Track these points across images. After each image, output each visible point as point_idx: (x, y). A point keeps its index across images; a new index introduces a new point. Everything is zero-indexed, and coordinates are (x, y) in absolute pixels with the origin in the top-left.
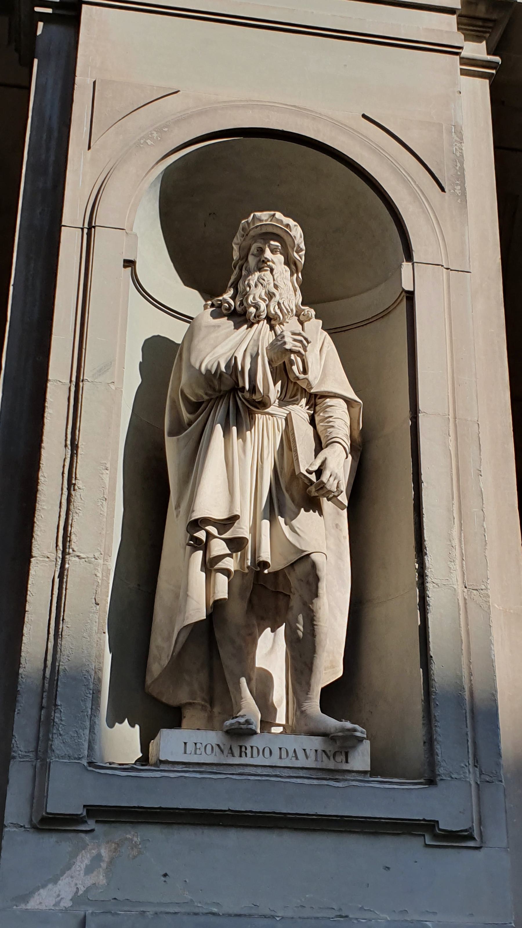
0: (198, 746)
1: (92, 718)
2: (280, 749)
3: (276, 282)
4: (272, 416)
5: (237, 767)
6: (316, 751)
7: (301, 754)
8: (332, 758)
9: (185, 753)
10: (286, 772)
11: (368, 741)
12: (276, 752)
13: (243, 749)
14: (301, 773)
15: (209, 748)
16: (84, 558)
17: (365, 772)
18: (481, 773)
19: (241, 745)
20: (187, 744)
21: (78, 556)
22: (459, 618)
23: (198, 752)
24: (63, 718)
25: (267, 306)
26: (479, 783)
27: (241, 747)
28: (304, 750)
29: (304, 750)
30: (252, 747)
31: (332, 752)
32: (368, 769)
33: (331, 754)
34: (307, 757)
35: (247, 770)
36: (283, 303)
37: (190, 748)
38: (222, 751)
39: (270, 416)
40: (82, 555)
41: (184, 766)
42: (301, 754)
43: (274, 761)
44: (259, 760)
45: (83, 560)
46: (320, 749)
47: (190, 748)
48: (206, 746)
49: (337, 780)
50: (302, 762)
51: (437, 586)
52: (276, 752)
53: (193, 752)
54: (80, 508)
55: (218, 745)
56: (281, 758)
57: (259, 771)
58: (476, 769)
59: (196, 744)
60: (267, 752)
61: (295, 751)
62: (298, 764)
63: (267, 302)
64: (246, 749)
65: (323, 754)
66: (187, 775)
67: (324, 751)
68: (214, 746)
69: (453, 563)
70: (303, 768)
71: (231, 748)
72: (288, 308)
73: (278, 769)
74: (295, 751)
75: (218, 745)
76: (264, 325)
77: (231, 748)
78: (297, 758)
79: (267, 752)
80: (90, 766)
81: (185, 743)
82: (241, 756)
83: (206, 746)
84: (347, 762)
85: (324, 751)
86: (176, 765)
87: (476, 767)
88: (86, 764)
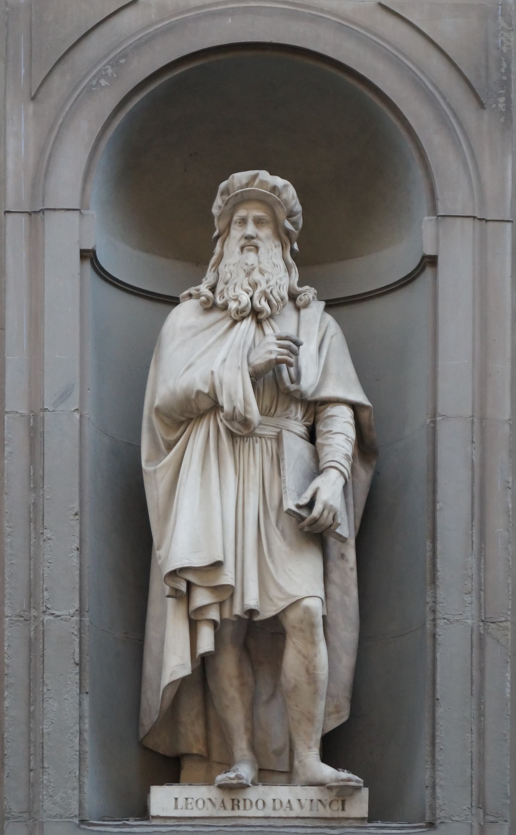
0: (190, 801)
1: (82, 778)
2: (274, 800)
3: (262, 266)
4: (260, 437)
5: (229, 819)
6: (312, 800)
7: (295, 805)
8: (328, 807)
9: (176, 807)
10: (280, 823)
11: (367, 789)
12: (269, 803)
13: (236, 802)
14: (297, 823)
15: (200, 803)
16: (59, 616)
17: (363, 819)
18: (485, 814)
19: (233, 798)
20: (179, 800)
21: (53, 614)
22: (472, 656)
23: (189, 806)
24: (52, 780)
25: (251, 298)
26: (482, 824)
27: (233, 800)
28: (299, 800)
29: (299, 800)
30: (245, 800)
31: (329, 801)
32: (366, 815)
33: (327, 804)
34: (302, 807)
35: (240, 822)
36: (271, 292)
37: (181, 803)
38: (214, 805)
39: (258, 439)
40: (57, 613)
41: (176, 820)
42: (295, 805)
43: (269, 812)
44: (253, 812)
45: (58, 618)
46: (315, 798)
47: (181, 803)
48: (197, 801)
49: (332, 828)
50: (297, 811)
51: (448, 623)
52: (269, 803)
53: (184, 807)
54: (50, 561)
55: (210, 799)
56: (274, 809)
57: (253, 822)
58: (481, 811)
59: (187, 799)
60: (260, 804)
61: (289, 801)
62: (293, 814)
63: (251, 294)
64: (239, 802)
65: (320, 804)
66: (179, 829)
67: (320, 801)
68: (206, 800)
69: (468, 596)
70: (297, 818)
71: (223, 802)
72: (278, 297)
73: (272, 820)
74: (289, 801)
75: (210, 799)
76: (247, 326)
77: (223, 802)
78: (291, 808)
79: (260, 804)
80: (83, 824)
81: (176, 799)
82: (233, 809)
83: (197, 801)
84: (343, 809)
85: (320, 801)
86: (168, 820)
87: (481, 808)
88: (77, 822)
